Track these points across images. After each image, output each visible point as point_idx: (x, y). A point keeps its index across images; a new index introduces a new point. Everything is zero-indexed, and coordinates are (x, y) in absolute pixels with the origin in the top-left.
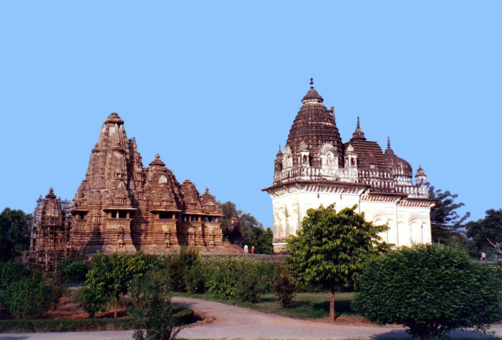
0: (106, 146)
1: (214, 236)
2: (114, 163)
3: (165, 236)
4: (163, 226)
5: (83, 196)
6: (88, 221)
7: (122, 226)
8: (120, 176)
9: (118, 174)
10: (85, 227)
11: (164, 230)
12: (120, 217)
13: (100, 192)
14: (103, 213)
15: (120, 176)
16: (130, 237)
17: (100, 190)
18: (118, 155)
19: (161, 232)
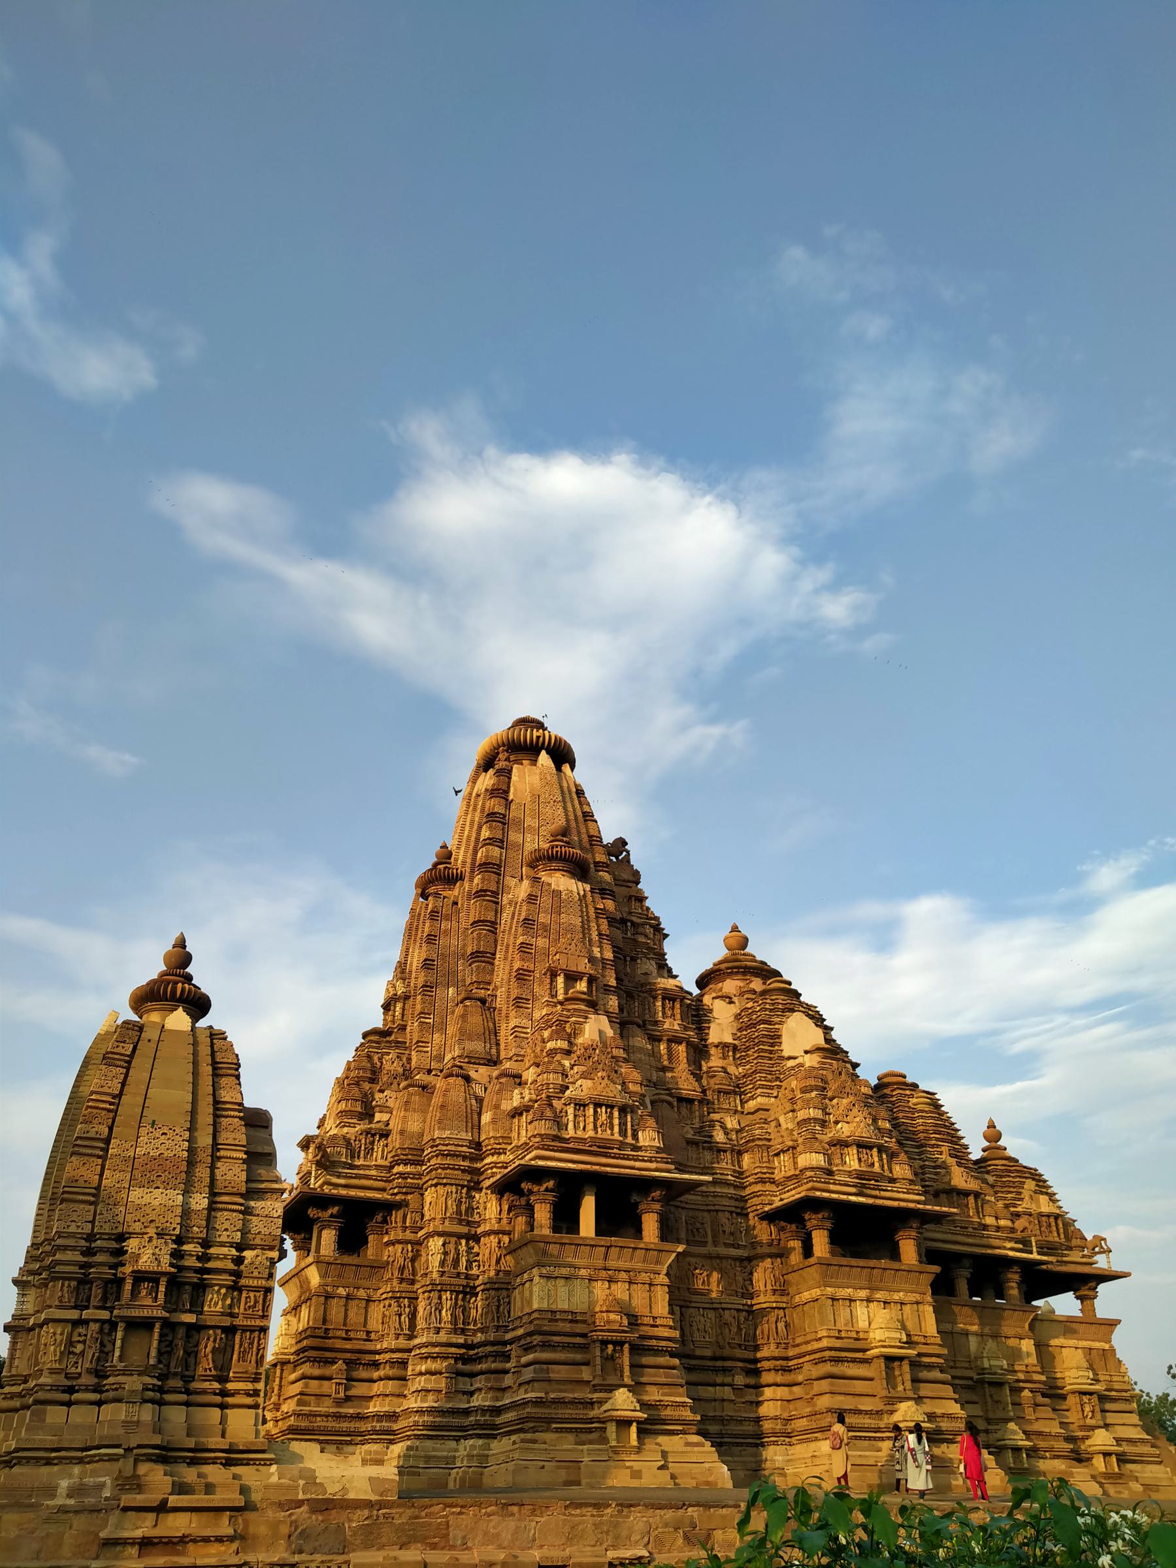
0: (500, 842)
1: (1102, 1398)
2: (543, 918)
3: (890, 1380)
4: (861, 1311)
5: (367, 1114)
6: (392, 1273)
7: (620, 1291)
8: (582, 986)
9: (572, 978)
10: (376, 1313)
11: (877, 1335)
12: (602, 1228)
13: (467, 1079)
14: (490, 1208)
15: (582, 986)
16: (677, 1376)
17: (472, 1074)
18: (563, 883)
19: (852, 1350)
